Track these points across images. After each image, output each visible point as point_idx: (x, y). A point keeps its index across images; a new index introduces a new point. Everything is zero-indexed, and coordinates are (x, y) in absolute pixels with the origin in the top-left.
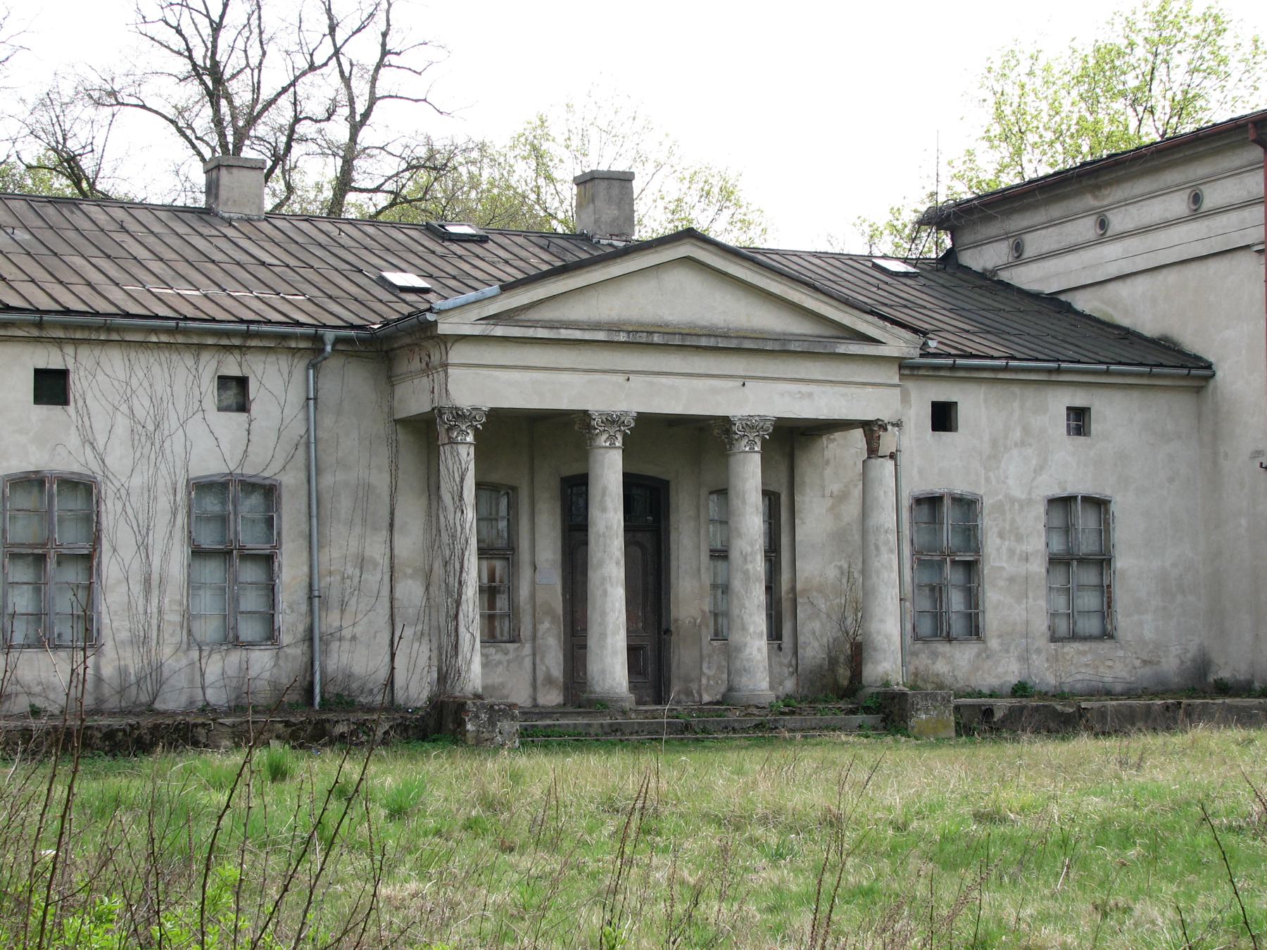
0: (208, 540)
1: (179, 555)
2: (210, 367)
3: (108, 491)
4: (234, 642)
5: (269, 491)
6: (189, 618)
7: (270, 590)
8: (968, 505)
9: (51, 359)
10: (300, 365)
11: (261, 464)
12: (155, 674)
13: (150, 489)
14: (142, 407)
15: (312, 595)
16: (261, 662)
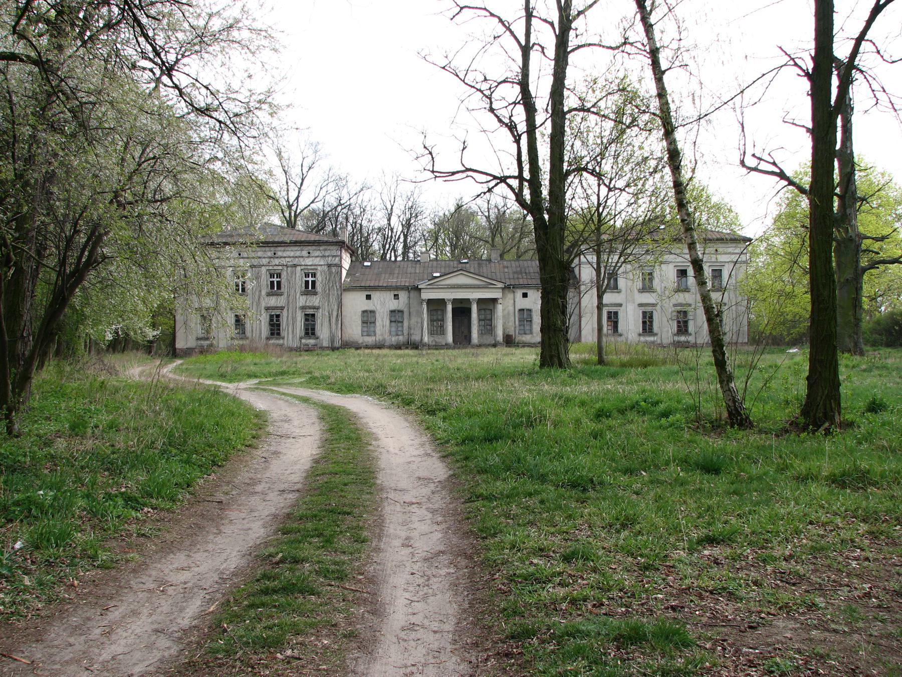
0: (393, 319)
1: (388, 322)
2: (392, 293)
3: (377, 313)
4: (397, 335)
5: (401, 312)
6: (390, 332)
7: (402, 327)
8: (530, 310)
9: (368, 293)
10: (407, 292)
11: (401, 307)
12: (384, 340)
13: (383, 312)
14: (382, 299)
15: (409, 328)
16: (401, 338)
